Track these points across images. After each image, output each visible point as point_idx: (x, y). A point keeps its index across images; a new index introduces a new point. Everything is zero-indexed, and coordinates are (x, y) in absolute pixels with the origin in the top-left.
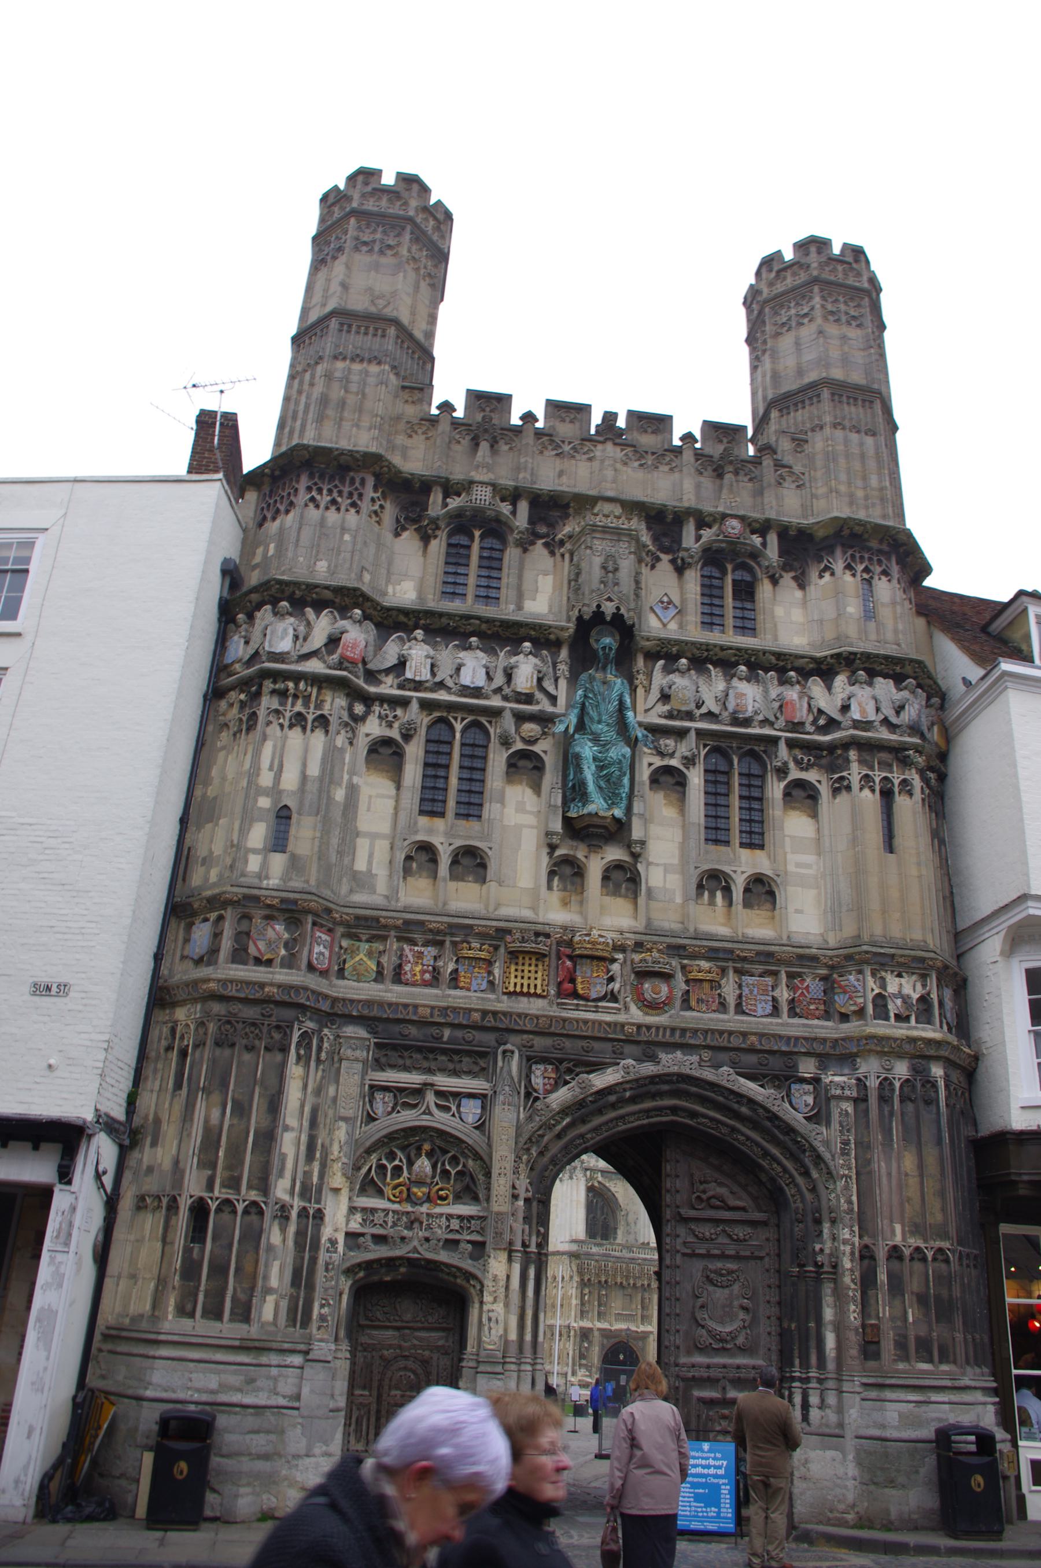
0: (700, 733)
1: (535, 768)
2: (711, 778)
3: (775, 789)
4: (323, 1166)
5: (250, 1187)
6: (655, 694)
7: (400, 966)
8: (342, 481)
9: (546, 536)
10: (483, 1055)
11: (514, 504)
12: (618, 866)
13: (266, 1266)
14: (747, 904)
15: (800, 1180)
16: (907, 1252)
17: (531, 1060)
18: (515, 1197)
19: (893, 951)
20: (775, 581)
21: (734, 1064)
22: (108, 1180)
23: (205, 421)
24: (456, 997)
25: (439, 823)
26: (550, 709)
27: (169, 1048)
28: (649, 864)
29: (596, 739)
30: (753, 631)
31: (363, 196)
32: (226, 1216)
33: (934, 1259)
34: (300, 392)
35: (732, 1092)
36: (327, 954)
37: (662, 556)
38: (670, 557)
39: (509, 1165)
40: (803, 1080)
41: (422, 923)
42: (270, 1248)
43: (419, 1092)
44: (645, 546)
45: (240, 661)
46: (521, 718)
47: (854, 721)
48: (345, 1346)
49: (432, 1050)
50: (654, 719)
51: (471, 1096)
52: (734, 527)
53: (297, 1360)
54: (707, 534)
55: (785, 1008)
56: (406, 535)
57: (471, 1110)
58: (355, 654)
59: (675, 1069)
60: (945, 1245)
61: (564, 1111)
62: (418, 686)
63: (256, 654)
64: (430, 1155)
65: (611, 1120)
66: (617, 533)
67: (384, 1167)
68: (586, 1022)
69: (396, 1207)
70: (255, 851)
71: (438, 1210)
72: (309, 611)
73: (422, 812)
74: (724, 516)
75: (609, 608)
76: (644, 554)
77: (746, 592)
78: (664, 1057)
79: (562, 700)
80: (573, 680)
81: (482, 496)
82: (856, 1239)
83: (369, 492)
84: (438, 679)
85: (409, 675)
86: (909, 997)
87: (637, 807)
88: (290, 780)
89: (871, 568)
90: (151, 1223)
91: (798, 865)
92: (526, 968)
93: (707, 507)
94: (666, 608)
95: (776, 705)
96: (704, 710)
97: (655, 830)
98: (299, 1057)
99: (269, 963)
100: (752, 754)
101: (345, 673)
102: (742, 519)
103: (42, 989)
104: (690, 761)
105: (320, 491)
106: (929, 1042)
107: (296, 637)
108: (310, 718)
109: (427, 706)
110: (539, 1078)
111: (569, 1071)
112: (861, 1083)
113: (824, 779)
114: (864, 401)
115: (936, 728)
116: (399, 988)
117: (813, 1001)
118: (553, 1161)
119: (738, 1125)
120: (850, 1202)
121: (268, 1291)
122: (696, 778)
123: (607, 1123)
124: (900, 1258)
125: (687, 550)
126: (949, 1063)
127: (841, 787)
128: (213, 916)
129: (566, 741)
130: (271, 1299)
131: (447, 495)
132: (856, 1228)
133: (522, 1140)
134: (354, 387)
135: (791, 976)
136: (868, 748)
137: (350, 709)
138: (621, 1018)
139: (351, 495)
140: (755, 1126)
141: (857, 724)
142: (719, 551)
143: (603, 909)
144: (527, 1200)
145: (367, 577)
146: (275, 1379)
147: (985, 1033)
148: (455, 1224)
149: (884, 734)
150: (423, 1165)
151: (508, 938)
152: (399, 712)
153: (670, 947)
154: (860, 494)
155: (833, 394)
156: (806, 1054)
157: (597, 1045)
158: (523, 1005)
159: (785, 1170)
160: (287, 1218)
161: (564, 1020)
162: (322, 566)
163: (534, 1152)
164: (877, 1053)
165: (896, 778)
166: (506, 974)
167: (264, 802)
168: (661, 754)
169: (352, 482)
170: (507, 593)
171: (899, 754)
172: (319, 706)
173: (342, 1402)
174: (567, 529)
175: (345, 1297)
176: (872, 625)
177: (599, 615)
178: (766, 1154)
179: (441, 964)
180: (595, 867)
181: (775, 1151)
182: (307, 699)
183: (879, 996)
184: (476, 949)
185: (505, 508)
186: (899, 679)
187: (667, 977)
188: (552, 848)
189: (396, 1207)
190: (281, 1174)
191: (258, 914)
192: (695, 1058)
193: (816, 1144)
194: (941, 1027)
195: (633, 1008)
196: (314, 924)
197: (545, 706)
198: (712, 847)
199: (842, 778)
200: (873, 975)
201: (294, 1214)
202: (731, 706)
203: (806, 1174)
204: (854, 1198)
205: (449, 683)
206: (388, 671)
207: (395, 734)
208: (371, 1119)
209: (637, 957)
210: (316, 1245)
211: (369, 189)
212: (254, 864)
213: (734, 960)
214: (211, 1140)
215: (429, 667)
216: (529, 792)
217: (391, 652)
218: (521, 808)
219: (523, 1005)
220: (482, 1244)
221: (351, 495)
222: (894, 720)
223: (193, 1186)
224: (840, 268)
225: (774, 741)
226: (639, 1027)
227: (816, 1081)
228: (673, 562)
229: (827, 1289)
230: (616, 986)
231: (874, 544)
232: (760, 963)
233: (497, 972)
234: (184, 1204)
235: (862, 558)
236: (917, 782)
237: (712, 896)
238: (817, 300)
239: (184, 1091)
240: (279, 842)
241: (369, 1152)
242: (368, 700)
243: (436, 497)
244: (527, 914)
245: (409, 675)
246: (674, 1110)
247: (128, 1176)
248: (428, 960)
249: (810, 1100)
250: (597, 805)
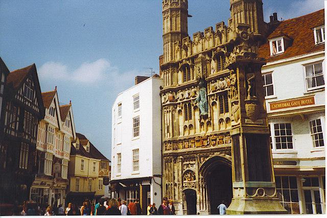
17: (200, 157)
50: (211, 93)
104: (216, 100)
122: (218, 102)
137: (174, 107)
138: (209, 148)
144: (202, 179)
145: (174, 83)
184: (192, 141)
185: (188, 62)
198: (221, 114)
207: (181, 109)
242: (177, 104)
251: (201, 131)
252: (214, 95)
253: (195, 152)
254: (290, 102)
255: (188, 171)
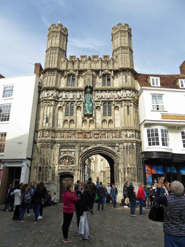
0: (102, 101)
1: (81, 108)
2: (104, 107)
3: (113, 107)
4: (55, 161)
5: (46, 165)
6: (96, 96)
7: (64, 136)
8: (52, 72)
9: (81, 76)
10: (75, 146)
11: (76, 72)
12: (92, 120)
13: (49, 174)
14: (109, 123)
15: (116, 159)
16: (130, 168)
18: (79, 164)
19: (128, 128)
20: (113, 78)
21: (107, 145)
22: (29, 166)
23: (36, 65)
24: (71, 139)
25: (68, 117)
26: (82, 100)
27: (36, 149)
28: (96, 119)
29: (88, 103)
30: (110, 85)
31: (53, 29)
32: (43, 168)
33: (134, 169)
34: (47, 59)
35: (107, 149)
36: (54, 135)
37: (97, 76)
38: (98, 76)
39: (78, 160)
40: (117, 146)
41: (66, 130)
42: (49, 172)
43: (67, 151)
44: (94, 75)
45: (41, 98)
46: (78, 102)
47: (123, 97)
48: (59, 183)
49: (68, 146)
50: (96, 100)
51: (73, 151)
52: (107, 71)
53: (53, 185)
54: (103, 72)
55: (114, 137)
56: (62, 78)
57: (73, 153)
58: (55, 96)
59: (99, 146)
60: (135, 167)
61: (85, 152)
62: (64, 99)
63: (43, 97)
64: (68, 159)
65: (91, 153)
66: (90, 75)
67: (63, 161)
68: (87, 141)
69: (64, 166)
70: (44, 123)
71: (70, 166)
72: (49, 91)
73: (66, 115)
74: (105, 70)
75: (88, 85)
76: (94, 77)
77: (109, 80)
78: (97, 144)
79: (83, 99)
80: (84, 96)
81: (71, 71)
82: (123, 166)
83: (56, 73)
84: (67, 98)
85: (63, 98)
86: (131, 134)
87: (94, 112)
88: (48, 114)
89: (127, 74)
90: (35, 170)
91: (116, 118)
92: (80, 135)
93: (102, 69)
94: (98, 84)
95: (113, 96)
96: (103, 98)
97: (97, 115)
98: (51, 149)
99: (47, 137)
100: (110, 103)
101: (54, 99)
102: (108, 69)
103: (19, 143)
104: (101, 105)
105: (50, 74)
106: (133, 140)
107: (47, 95)
108: (50, 105)
109: (65, 101)
110: (82, 148)
111: (86, 147)
112: (124, 147)
113: (120, 105)
114: (126, 49)
115: (136, 96)
116: (63, 139)
117: (118, 136)
118: (84, 159)
119: (108, 153)
120: (122, 162)
121: (49, 177)
122: (102, 107)
123: (91, 154)
124: (129, 169)
125: (100, 75)
126: (136, 143)
127: (122, 106)
128: (40, 132)
129: (84, 104)
130: (49, 178)
131: (67, 72)
132: (123, 165)
133: (79, 157)
134: (54, 58)
135: (115, 133)
136: (125, 101)
137: (56, 103)
138: (92, 140)
139: (54, 74)
140: (110, 153)
141: (124, 97)
142: (105, 75)
143: (89, 126)
144: (81, 164)
146: (50, 187)
147: (142, 138)
148: (72, 167)
149: (128, 99)
150: (67, 160)
151: (77, 131)
152: (62, 103)
153: (98, 130)
154: (126, 63)
155: (122, 48)
156: (117, 143)
157: (89, 144)
158: (79, 139)
159: (114, 158)
160: (51, 168)
161: (84, 141)
162: (51, 84)
163: (81, 158)
164: (126, 142)
165: (129, 104)
166: (77, 136)
167: (45, 117)
168: (97, 104)
169: (54, 71)
170: (76, 84)
171: (129, 100)
172: (51, 103)
173: (59, 189)
174: (84, 74)
175: (59, 177)
176: (127, 83)
177: (87, 87)
178: (112, 156)
179: (69, 135)
180: (88, 120)
181: (113, 156)
182: (50, 102)
183: (127, 135)
184: (73, 133)
185: (75, 73)
186: (130, 90)
187: (98, 134)
188: (83, 119)
189: (64, 166)
190: (50, 163)
191: (45, 131)
192: (102, 145)
193: (118, 155)
194: (135, 138)
195: (94, 138)
196: (52, 132)
197: (81, 100)
198: (104, 116)
199: (122, 105)
200: (126, 131)
201: (52, 168)
202: (106, 97)
203: (117, 158)
204: (123, 161)
205: (68, 98)
206: (60, 97)
207: (62, 106)
208: (61, 155)
209: (94, 132)
210: (55, 171)
211: (54, 27)
212: (44, 125)
213: (107, 131)
214: (41, 159)
215: (65, 96)
216: (80, 111)
217: (61, 95)
218: (79, 114)
219: (79, 139)
220: (75, 170)
221: (54, 74)
222: (129, 96)
223: (39, 165)
224: (123, 28)
225: (112, 101)
226: (94, 141)
227: (118, 146)
228: (99, 77)
229: (120, 173)
230: (91, 136)
231: (127, 71)
232: (111, 131)
233: (76, 135)
234: (38, 167)
235: (125, 73)
236: (132, 104)
237: (104, 122)
238: (120, 34)
239: (38, 154)
240: (47, 122)
241: (61, 159)
242: (58, 102)
243: (65, 72)
244: (80, 127)
245: (63, 98)
246: (100, 151)
247: (32, 165)
248: (67, 135)
249: (118, 149)
250: (88, 112)
251: (82, 126)
252: (100, 101)
253: (76, 142)
254: (176, 116)
255: (65, 157)
